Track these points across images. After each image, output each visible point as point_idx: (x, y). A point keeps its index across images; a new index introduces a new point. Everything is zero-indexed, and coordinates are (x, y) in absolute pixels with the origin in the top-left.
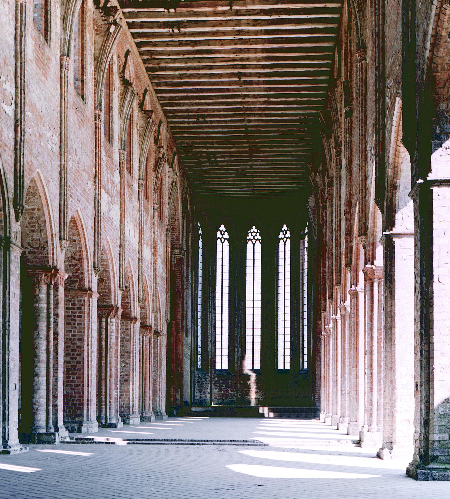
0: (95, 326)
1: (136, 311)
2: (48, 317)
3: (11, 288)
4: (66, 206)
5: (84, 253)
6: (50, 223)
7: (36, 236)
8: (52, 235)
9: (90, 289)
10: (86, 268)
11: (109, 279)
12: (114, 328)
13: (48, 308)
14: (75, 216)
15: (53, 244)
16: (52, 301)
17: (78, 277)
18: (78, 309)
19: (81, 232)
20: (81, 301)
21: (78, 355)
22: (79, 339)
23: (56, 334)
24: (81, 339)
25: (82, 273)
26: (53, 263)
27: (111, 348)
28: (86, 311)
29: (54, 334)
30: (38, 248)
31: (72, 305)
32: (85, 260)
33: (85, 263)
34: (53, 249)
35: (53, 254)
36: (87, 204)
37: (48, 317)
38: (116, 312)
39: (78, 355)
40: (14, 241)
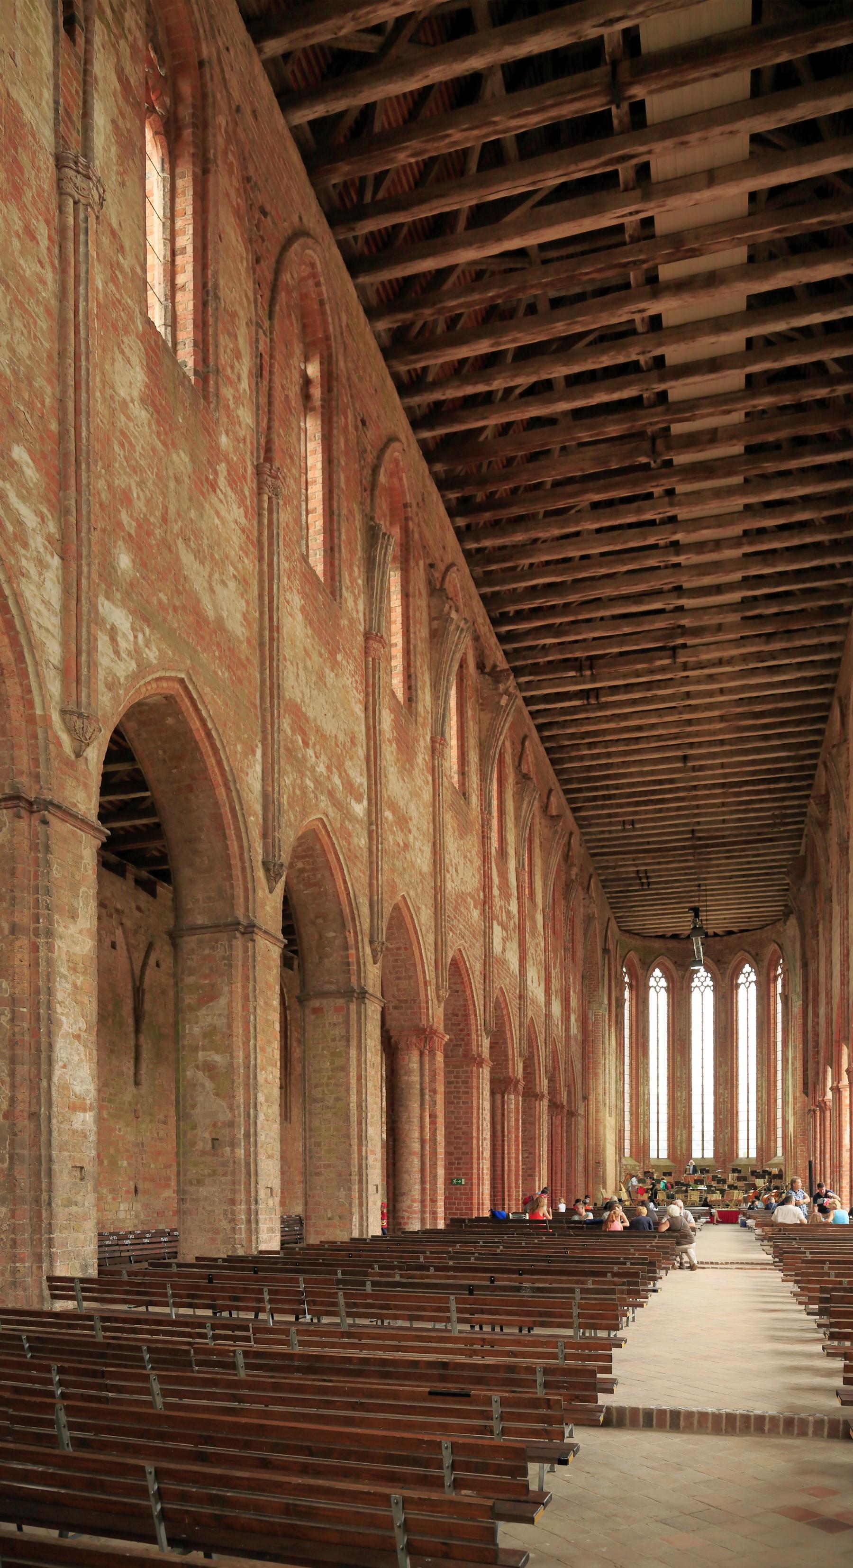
0: (487, 1105)
1: (543, 1084)
2: (422, 1094)
3: (369, 1054)
4: (444, 943)
5: (471, 1007)
6: (423, 967)
7: (403, 984)
8: (425, 983)
9: (480, 1056)
10: (474, 1027)
11: (505, 1042)
12: (513, 1106)
13: (422, 1083)
14: (458, 957)
15: (427, 995)
16: (427, 1072)
17: (463, 1040)
18: (463, 1082)
19: (466, 979)
20: (467, 1072)
21: (464, 1144)
22: (466, 1123)
23: (433, 1117)
24: (469, 1123)
25: (469, 1035)
26: (428, 1020)
27: (509, 1132)
28: (475, 1084)
29: (430, 1116)
30: (406, 1001)
31: (455, 1077)
32: (472, 1017)
33: (473, 1022)
34: (427, 1002)
35: (428, 1008)
36: (474, 941)
37: (422, 1094)
38: (516, 1087)
39: (464, 1144)
40: (371, 991)
